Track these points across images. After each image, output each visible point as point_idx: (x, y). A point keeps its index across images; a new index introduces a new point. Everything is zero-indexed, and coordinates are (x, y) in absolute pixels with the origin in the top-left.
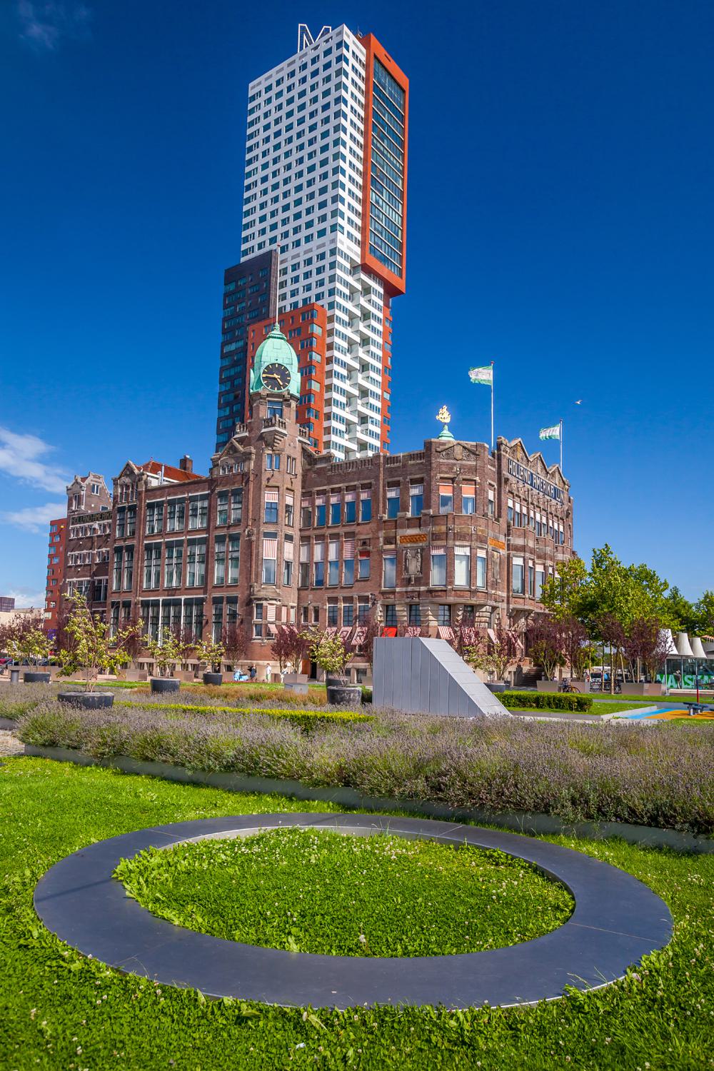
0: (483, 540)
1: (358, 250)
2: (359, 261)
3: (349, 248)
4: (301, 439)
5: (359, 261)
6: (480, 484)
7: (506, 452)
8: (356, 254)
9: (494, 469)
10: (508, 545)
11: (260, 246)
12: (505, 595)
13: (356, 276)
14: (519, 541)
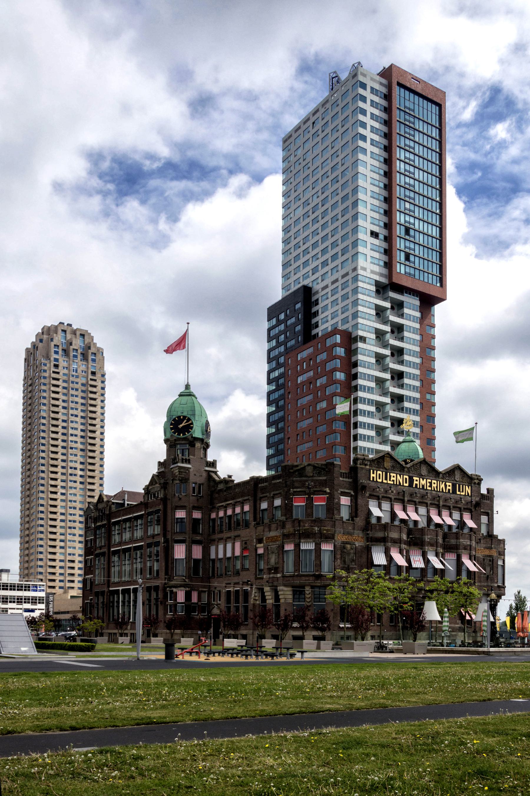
0: (329, 538)
2: (384, 280)
13: (386, 296)
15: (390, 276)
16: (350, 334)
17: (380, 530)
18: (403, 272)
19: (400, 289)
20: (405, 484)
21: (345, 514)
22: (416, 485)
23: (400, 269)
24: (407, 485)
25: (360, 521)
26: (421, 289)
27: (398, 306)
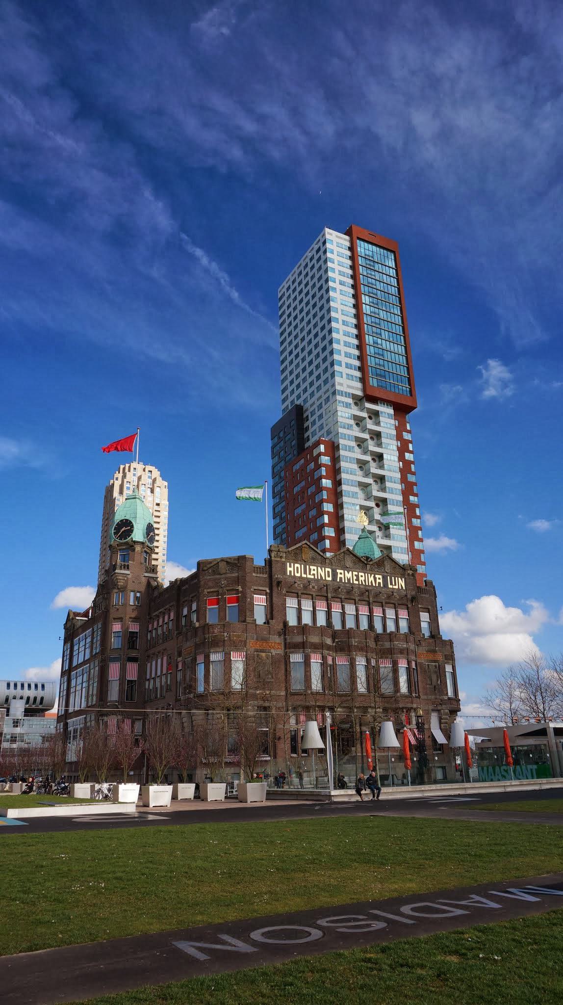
0: (238, 646)
1: (359, 385)
2: (360, 393)
3: (348, 386)
4: (146, 575)
5: (360, 393)
6: (241, 592)
7: (281, 557)
8: (357, 389)
9: (265, 576)
10: (285, 644)
11: (292, 402)
12: (283, 693)
14: (298, 639)
15: (364, 389)
16: (333, 443)
17: (298, 634)
18: (375, 385)
19: (374, 400)
20: (328, 579)
21: (260, 616)
22: (341, 578)
23: (373, 382)
24: (330, 579)
25: (277, 625)
26: (392, 399)
27: (374, 415)
